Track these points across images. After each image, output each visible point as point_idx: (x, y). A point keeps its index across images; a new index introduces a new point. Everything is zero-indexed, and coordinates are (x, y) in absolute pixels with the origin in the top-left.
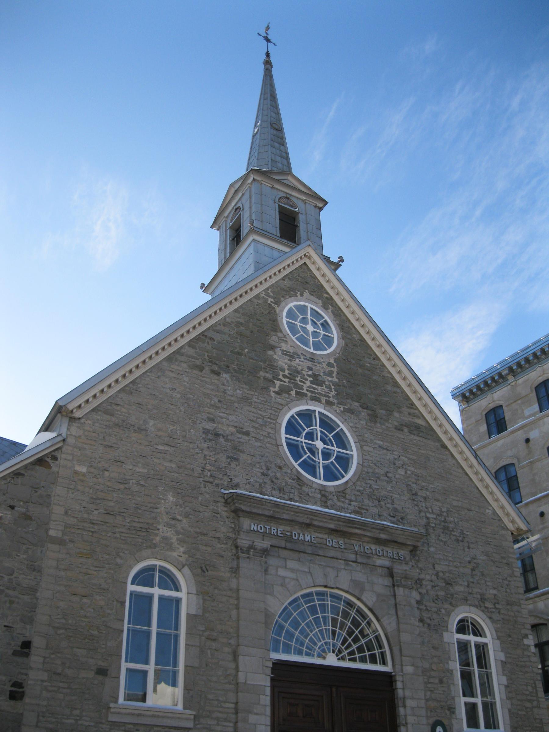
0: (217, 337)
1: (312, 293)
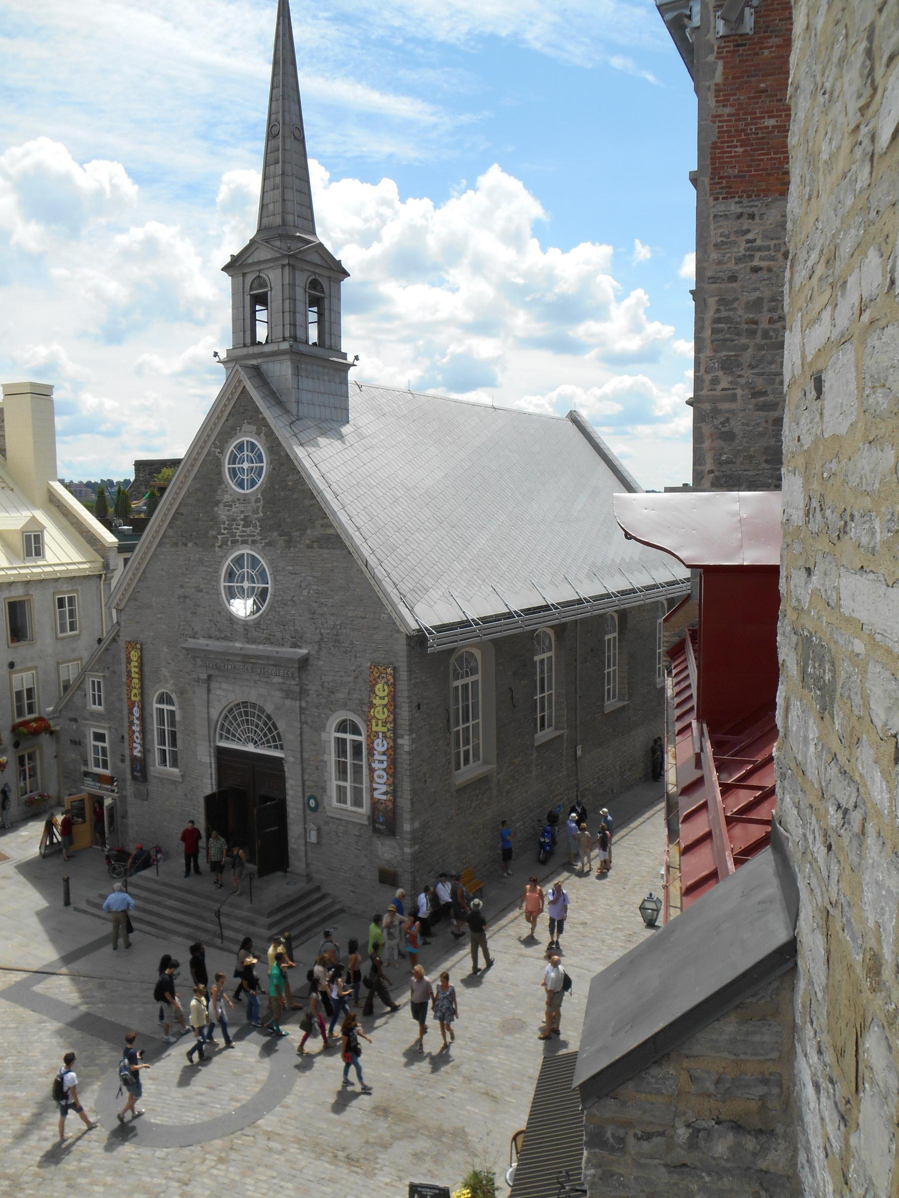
0: (184, 510)
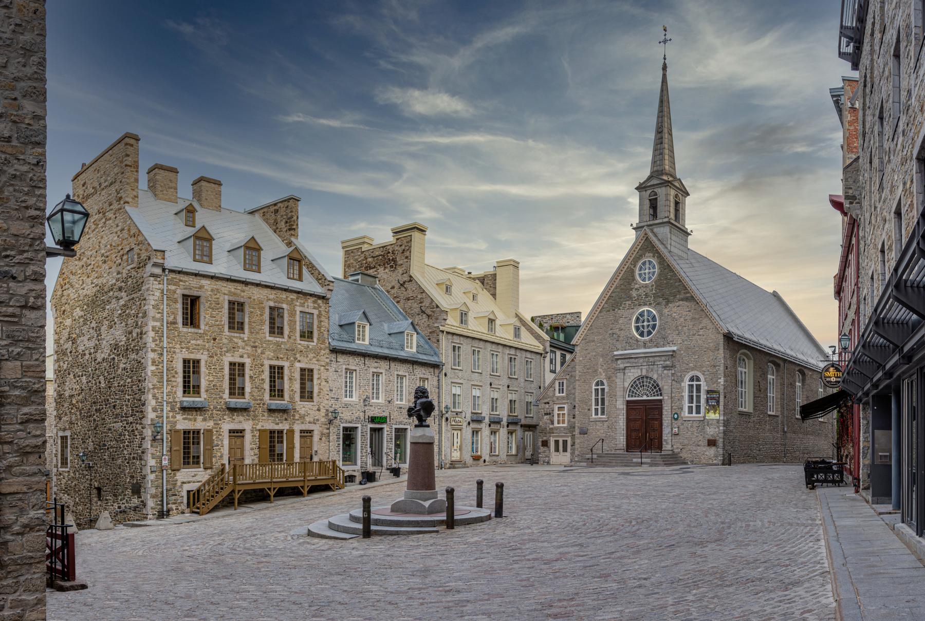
0: (614, 295)
1: (650, 251)
